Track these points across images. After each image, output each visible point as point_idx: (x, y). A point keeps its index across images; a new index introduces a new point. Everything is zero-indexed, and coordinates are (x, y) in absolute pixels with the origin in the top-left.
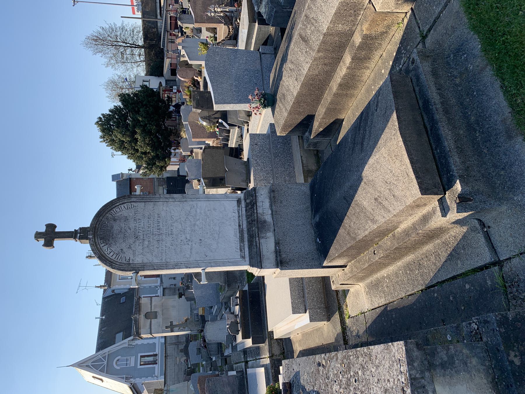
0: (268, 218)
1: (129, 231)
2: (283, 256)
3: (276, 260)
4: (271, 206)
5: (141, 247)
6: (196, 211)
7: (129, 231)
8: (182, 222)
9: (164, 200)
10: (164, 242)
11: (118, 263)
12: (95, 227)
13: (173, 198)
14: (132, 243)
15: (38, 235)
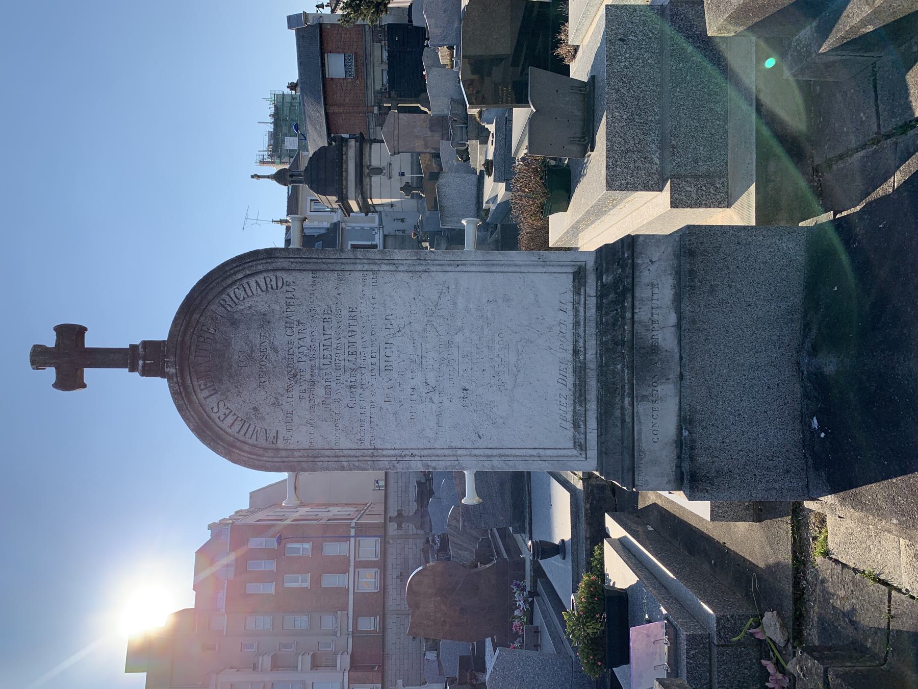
0: (666, 339)
1: (272, 356)
2: (700, 460)
3: (679, 467)
4: (678, 299)
5: (306, 404)
6: (455, 304)
7: (272, 356)
8: (416, 336)
9: (367, 267)
10: (367, 393)
11: (247, 448)
12: (183, 341)
13: (391, 262)
14: (281, 391)
15: (40, 357)
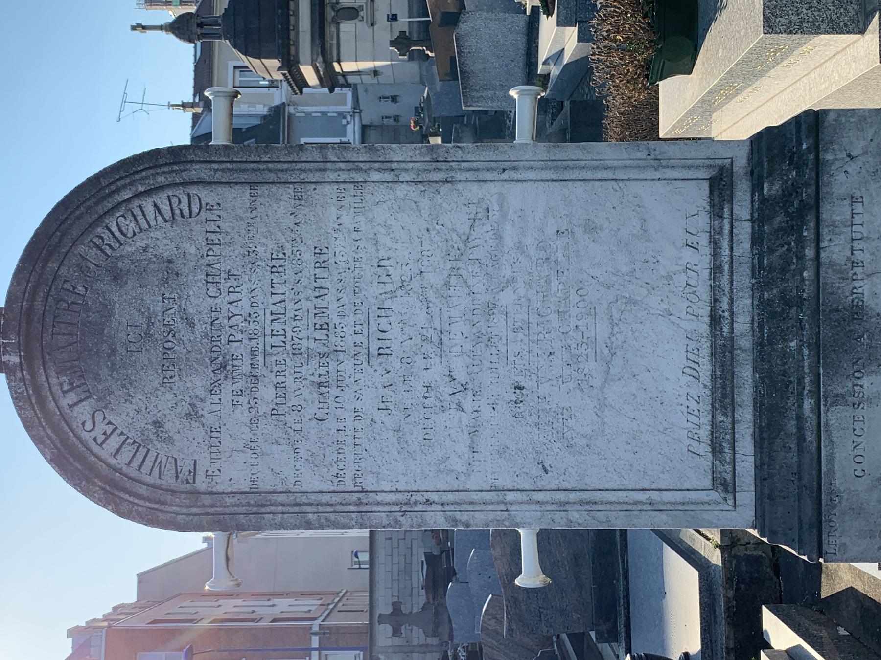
5: (242, 415)
6: (499, 237)
9: (344, 176)
10: (348, 394)
11: (143, 490)
12: (30, 309)
13: (386, 166)
14: (201, 392)
